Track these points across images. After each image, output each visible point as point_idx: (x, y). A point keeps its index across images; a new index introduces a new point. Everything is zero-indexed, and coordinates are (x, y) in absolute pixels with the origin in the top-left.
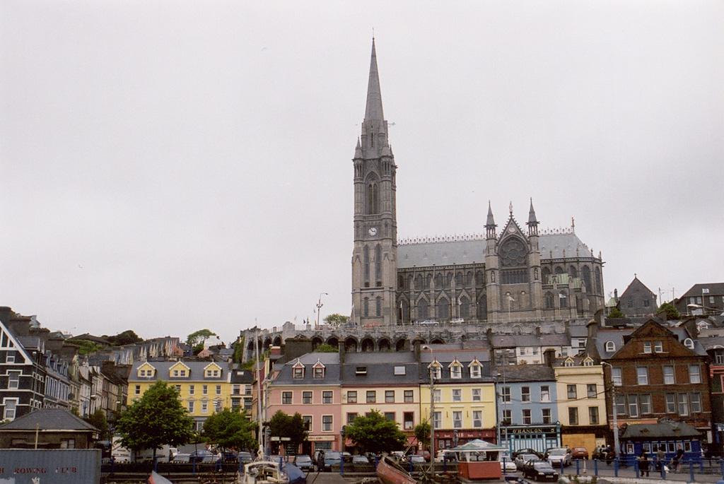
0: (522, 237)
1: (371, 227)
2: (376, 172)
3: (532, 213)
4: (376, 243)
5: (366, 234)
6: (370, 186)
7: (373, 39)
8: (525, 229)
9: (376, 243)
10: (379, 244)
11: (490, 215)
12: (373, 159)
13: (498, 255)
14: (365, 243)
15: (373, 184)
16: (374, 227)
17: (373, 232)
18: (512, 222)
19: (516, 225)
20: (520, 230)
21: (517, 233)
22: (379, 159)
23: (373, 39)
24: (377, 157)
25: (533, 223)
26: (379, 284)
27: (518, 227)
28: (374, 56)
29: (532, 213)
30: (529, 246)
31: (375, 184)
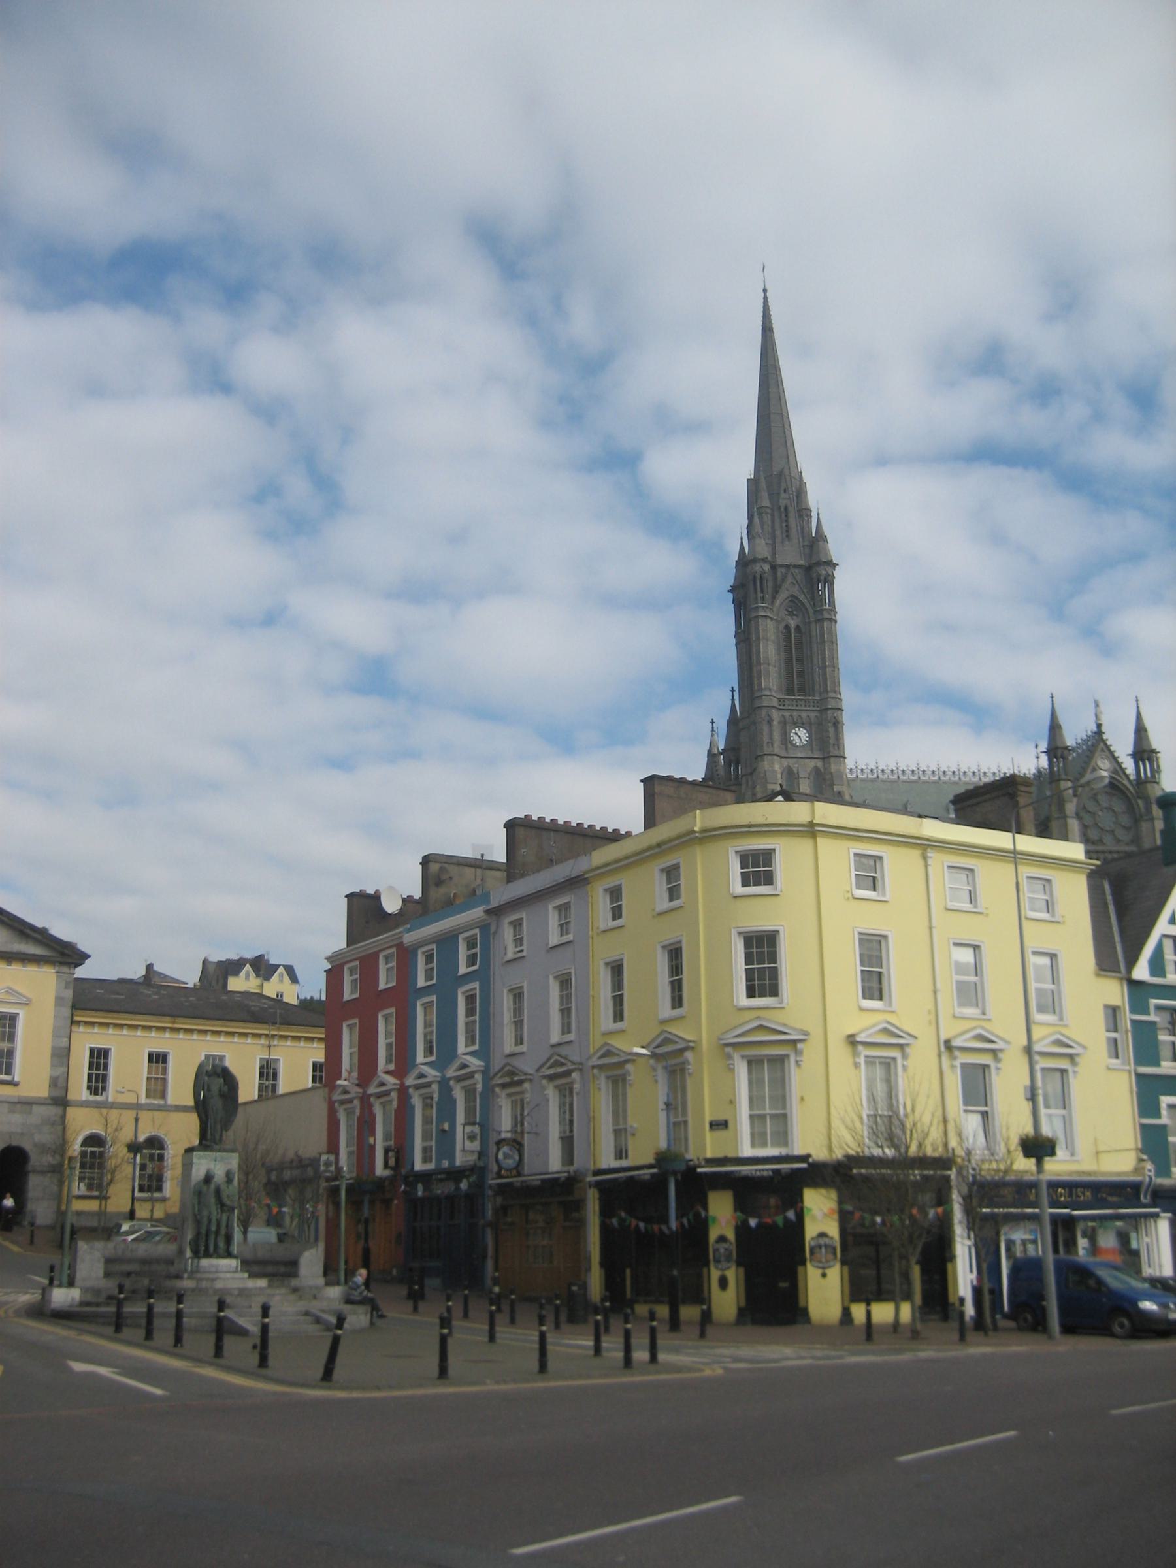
0: (1125, 782)
1: (796, 724)
2: (802, 598)
3: (1140, 731)
4: (812, 764)
5: (786, 741)
6: (787, 627)
7: (765, 291)
8: (1129, 765)
9: (812, 764)
10: (816, 770)
11: (1055, 728)
12: (796, 566)
13: (1078, 816)
14: (785, 762)
15: (793, 623)
16: (802, 725)
17: (800, 736)
18: (1097, 741)
19: (1112, 753)
20: (1119, 765)
21: (1115, 772)
22: (808, 569)
23: (765, 291)
24: (802, 562)
25: (1143, 752)
27: (1115, 759)
28: (767, 329)
29: (1140, 731)
30: (1140, 802)
31: (798, 628)
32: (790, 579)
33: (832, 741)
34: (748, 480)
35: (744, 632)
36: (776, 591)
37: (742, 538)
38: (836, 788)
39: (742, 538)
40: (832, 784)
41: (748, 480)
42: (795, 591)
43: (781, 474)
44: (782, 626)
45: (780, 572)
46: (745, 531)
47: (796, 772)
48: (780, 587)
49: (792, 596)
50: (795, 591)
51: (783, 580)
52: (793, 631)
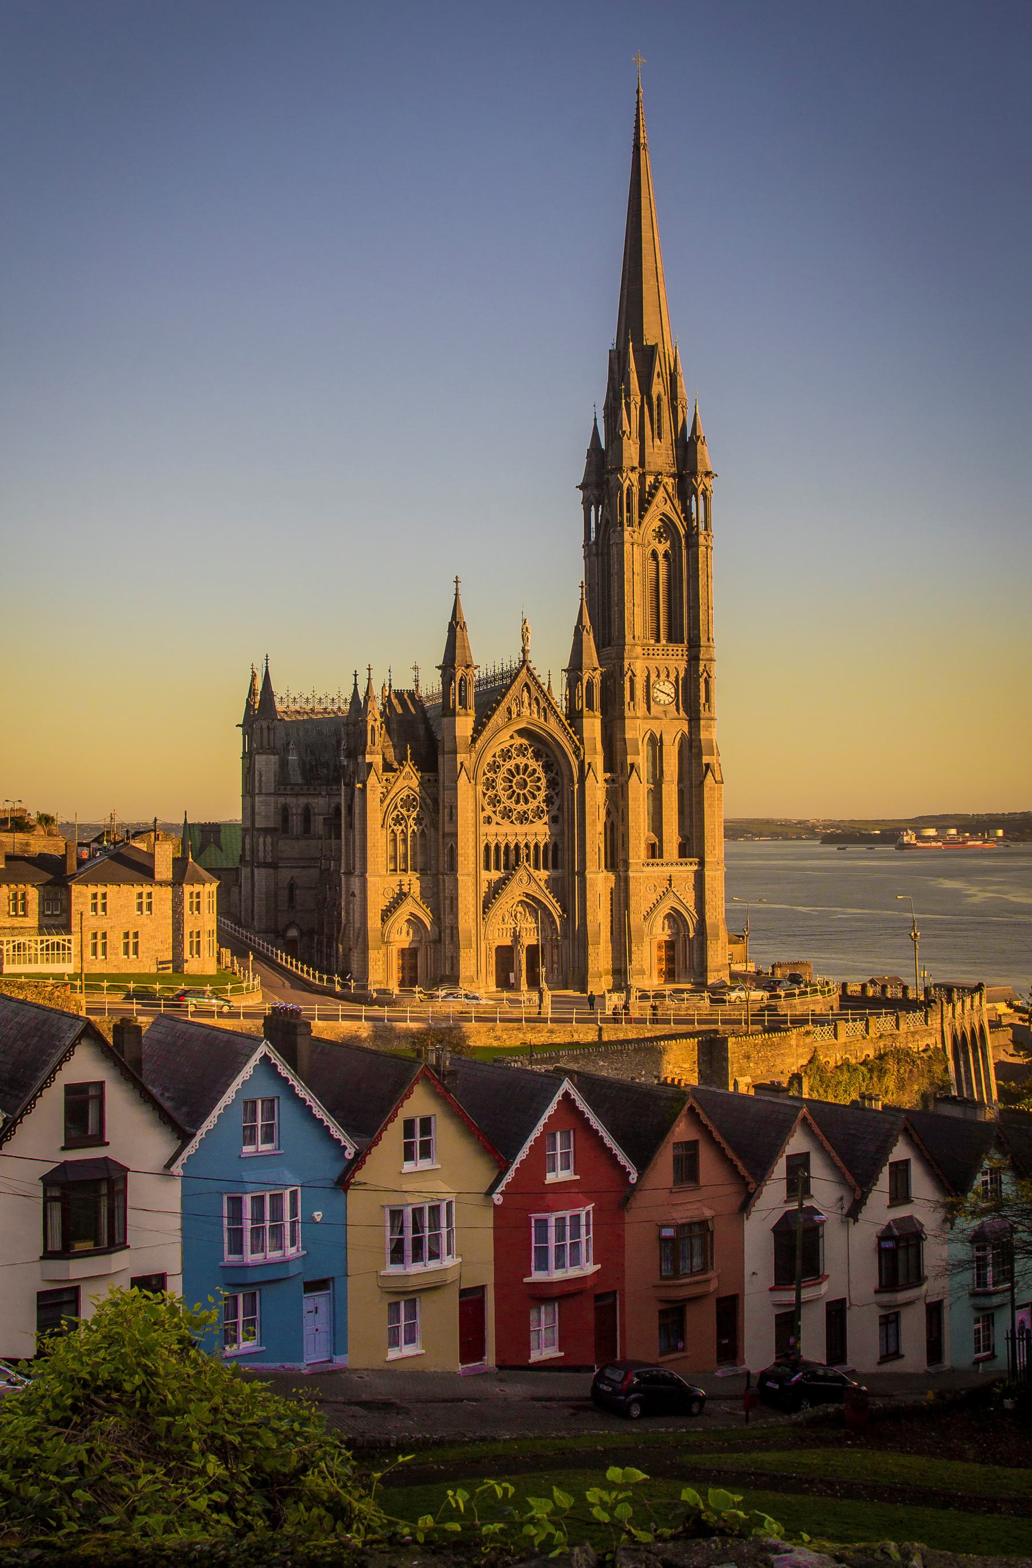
6: (654, 555)
26: (684, 851)
31: (666, 555)
32: (661, 494)
33: (702, 700)
34: (610, 351)
35: (596, 543)
36: (645, 504)
37: (595, 420)
38: (706, 759)
39: (595, 420)
40: (700, 755)
41: (610, 351)
42: (667, 509)
43: (653, 349)
44: (648, 552)
45: (650, 479)
46: (600, 416)
47: (658, 737)
48: (649, 503)
49: (663, 514)
50: (667, 509)
51: (653, 496)
52: (660, 558)
